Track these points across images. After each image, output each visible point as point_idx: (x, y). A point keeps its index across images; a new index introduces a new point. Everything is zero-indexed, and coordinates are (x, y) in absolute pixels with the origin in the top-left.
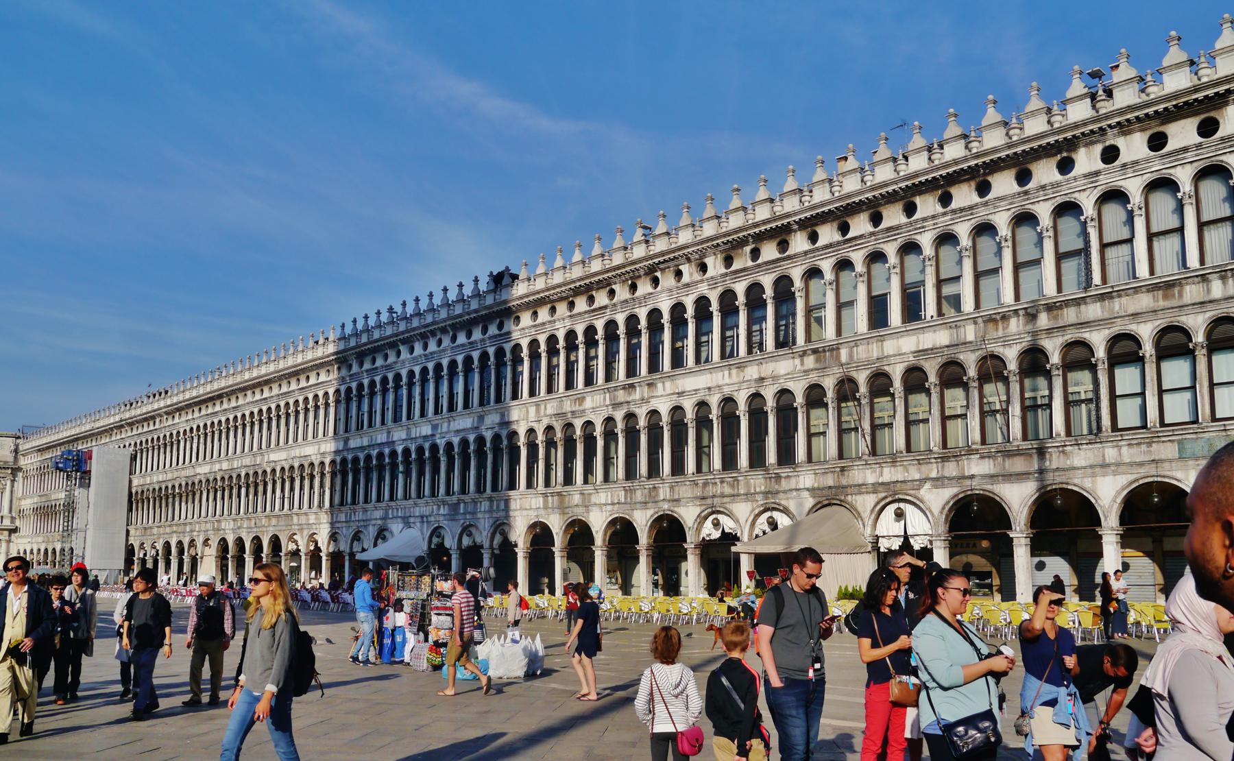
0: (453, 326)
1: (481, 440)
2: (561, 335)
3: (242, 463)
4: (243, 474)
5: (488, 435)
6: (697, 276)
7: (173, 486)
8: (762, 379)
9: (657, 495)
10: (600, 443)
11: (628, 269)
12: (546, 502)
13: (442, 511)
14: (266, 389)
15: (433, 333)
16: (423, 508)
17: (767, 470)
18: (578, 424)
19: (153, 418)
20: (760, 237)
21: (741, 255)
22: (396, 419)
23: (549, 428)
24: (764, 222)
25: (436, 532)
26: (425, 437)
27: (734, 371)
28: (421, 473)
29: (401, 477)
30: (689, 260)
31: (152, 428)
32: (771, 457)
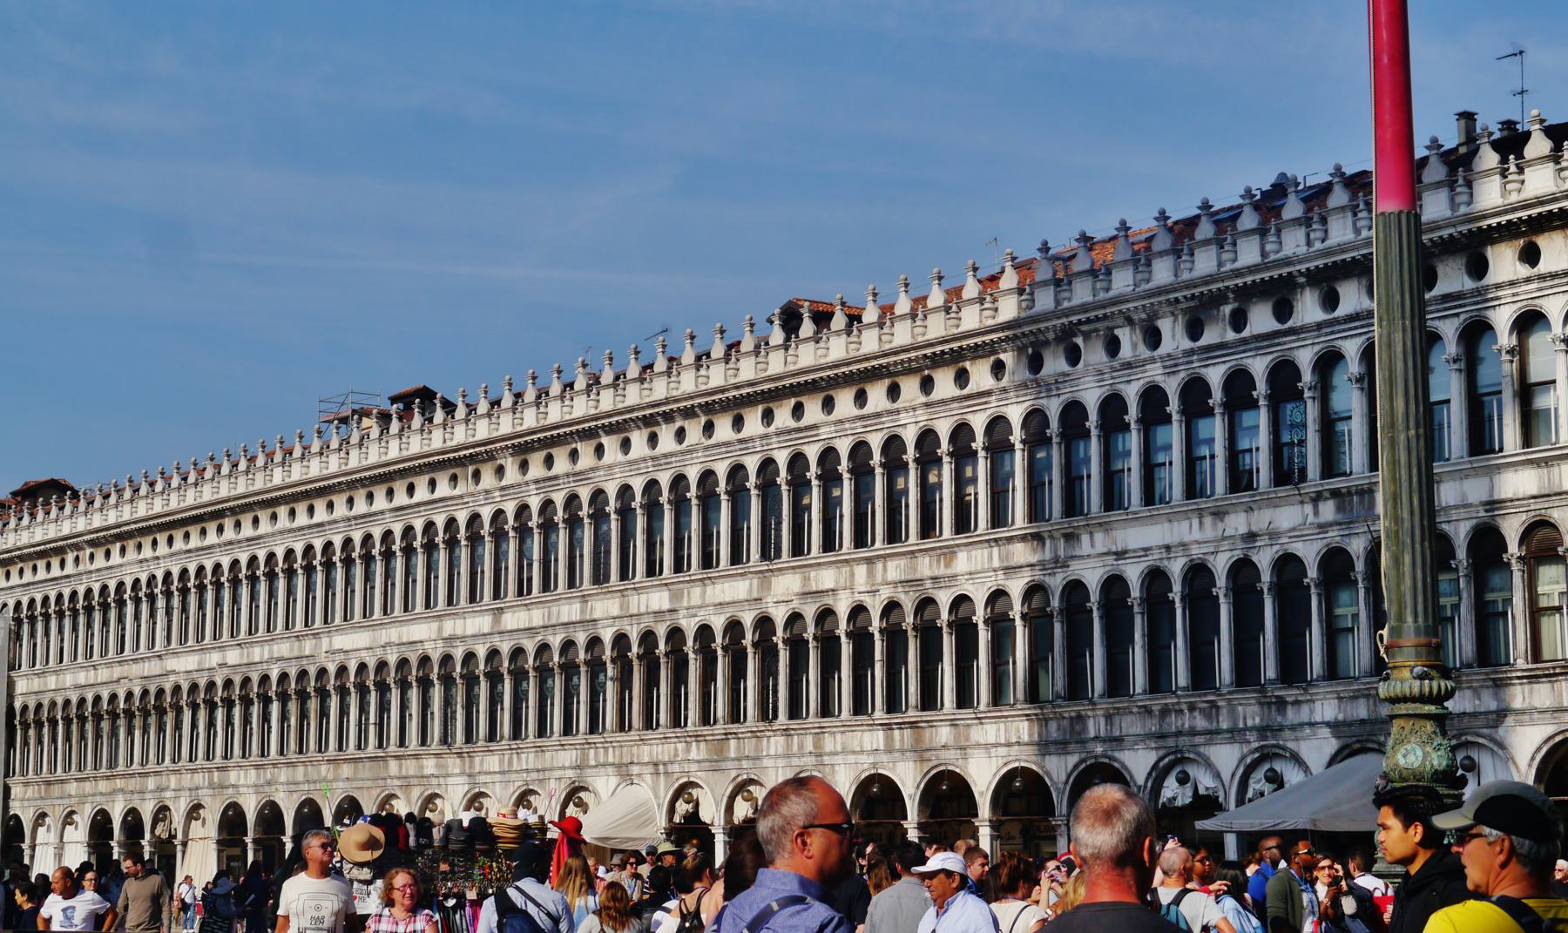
0: (708, 408)
1: (765, 623)
2: (910, 436)
3: (272, 654)
4: (274, 676)
5: (780, 616)
6: (1144, 352)
7: (113, 697)
8: (1251, 536)
9: (1085, 729)
10: (984, 636)
11: (1026, 329)
12: (889, 740)
13: (693, 755)
14: (320, 505)
15: (668, 417)
16: (659, 747)
18: (944, 599)
19: (60, 551)
20: (1248, 294)
21: (1215, 319)
22: (600, 577)
23: (892, 607)
24: (1252, 269)
25: (683, 790)
26: (658, 613)
27: (1208, 520)
28: (651, 682)
30: (1130, 321)
31: (56, 571)
32: (1270, 670)
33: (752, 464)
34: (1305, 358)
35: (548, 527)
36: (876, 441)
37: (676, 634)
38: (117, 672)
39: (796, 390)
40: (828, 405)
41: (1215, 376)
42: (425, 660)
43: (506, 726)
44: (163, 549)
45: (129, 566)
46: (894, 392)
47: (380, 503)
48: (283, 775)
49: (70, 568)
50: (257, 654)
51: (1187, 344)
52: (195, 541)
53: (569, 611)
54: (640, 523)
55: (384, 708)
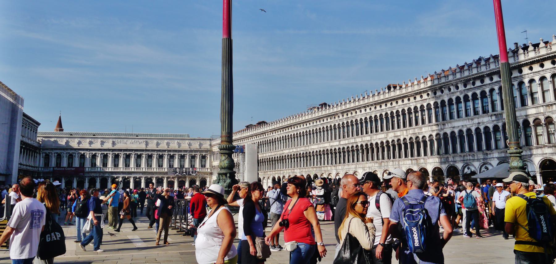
0: (375, 104)
1: (387, 142)
2: (412, 108)
3: (302, 150)
5: (390, 140)
6: (456, 90)
8: (479, 123)
10: (428, 143)
12: (412, 162)
15: (368, 106)
17: (483, 152)
18: (421, 137)
19: (265, 133)
20: (475, 79)
22: (357, 134)
23: (411, 138)
24: (476, 74)
27: (470, 121)
28: (368, 153)
29: (360, 154)
30: (453, 85)
33: (384, 114)
34: (487, 90)
35: (348, 126)
36: (406, 109)
37: (371, 144)
38: (275, 153)
39: (391, 100)
40: (397, 102)
41: (470, 94)
42: (327, 150)
43: (342, 161)
44: (282, 132)
45: (276, 135)
46: (409, 100)
47: (318, 123)
48: (304, 170)
49: (267, 136)
50: (299, 149)
51: (464, 89)
52: (287, 131)
53: (352, 141)
54: (364, 125)
55: (321, 158)
